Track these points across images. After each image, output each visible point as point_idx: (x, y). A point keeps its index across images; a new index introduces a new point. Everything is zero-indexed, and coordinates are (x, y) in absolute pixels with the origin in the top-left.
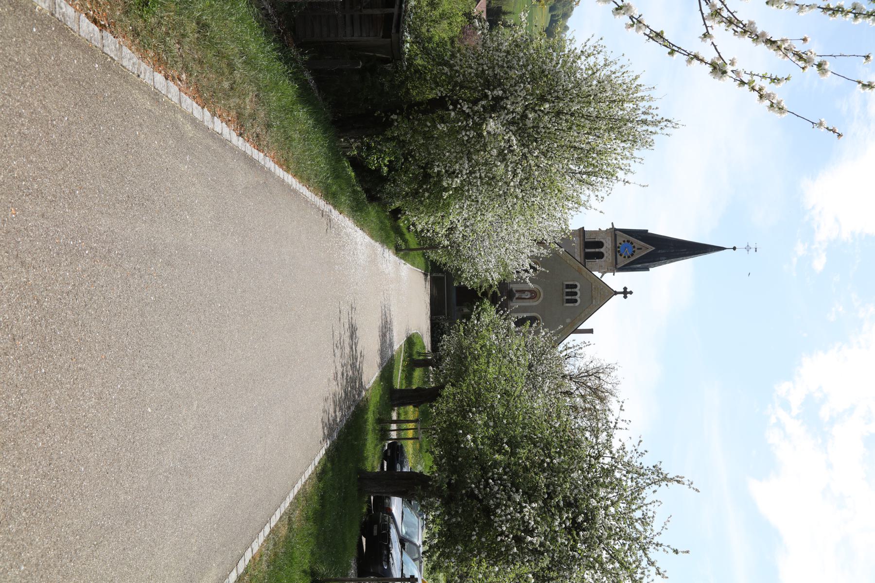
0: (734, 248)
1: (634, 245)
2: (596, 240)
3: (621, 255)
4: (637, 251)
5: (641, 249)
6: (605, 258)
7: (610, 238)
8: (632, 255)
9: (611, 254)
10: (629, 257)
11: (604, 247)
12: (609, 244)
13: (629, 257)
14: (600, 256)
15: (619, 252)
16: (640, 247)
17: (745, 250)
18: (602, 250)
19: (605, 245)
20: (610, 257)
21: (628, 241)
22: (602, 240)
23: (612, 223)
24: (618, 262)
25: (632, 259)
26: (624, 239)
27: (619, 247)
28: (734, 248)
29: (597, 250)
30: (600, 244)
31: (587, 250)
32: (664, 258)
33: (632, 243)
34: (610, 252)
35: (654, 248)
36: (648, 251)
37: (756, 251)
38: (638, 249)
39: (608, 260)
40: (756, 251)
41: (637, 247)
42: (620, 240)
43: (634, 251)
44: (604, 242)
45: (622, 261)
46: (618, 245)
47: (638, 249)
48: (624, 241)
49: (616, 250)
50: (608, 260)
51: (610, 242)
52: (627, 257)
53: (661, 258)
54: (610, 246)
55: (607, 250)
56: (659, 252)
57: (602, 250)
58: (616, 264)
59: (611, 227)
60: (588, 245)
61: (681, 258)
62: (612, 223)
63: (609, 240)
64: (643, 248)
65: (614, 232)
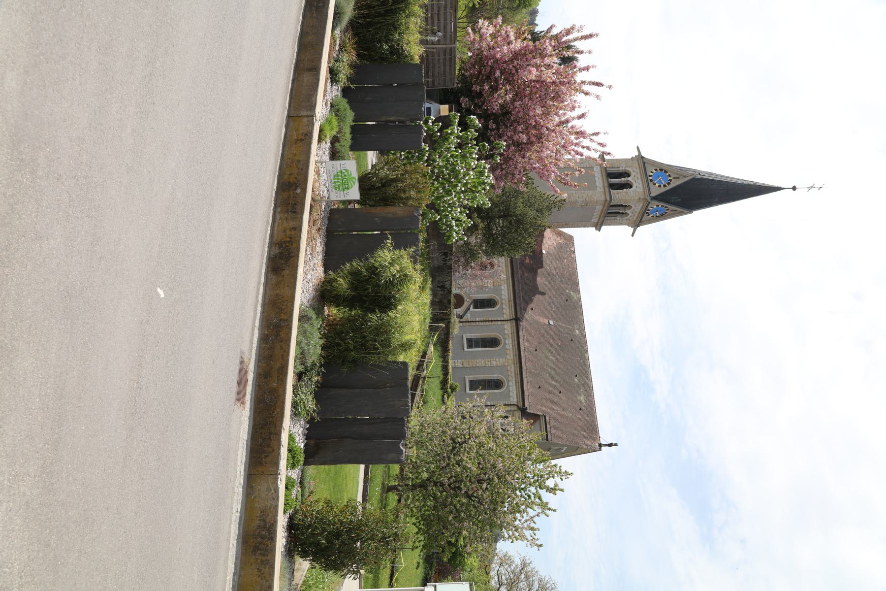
0: (794, 188)
2: (621, 169)
5: (679, 178)
6: (634, 188)
8: (669, 184)
9: (640, 182)
11: (632, 176)
13: (665, 186)
14: (628, 186)
15: (651, 180)
16: (676, 176)
18: (629, 179)
19: (633, 174)
20: (641, 186)
21: (661, 170)
22: (628, 169)
23: (638, 148)
25: (668, 188)
26: (656, 168)
27: (650, 176)
28: (794, 188)
29: (623, 179)
30: (627, 175)
33: (666, 172)
34: (640, 181)
38: (674, 178)
41: (673, 175)
44: (631, 171)
47: (674, 178)
48: (656, 170)
50: (638, 190)
51: (638, 170)
55: (636, 179)
58: (650, 193)
59: (637, 154)
60: (611, 175)
62: (638, 148)
64: (681, 177)
65: (641, 161)
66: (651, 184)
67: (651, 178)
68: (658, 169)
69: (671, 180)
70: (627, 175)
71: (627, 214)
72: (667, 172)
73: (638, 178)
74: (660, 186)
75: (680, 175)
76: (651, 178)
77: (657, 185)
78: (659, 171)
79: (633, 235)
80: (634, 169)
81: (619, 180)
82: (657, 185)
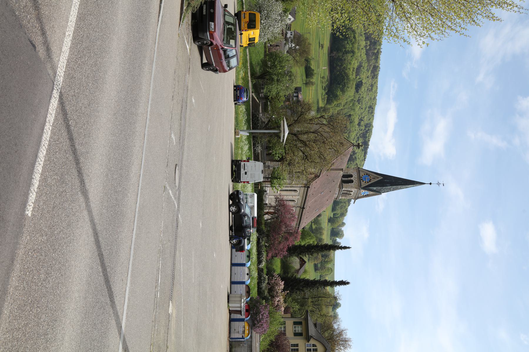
0: (430, 184)
1: (370, 176)
2: (348, 173)
3: (363, 181)
4: (372, 179)
5: (375, 178)
6: (354, 183)
7: (356, 172)
8: (370, 181)
10: (368, 182)
11: (353, 177)
12: (356, 176)
13: (368, 182)
14: (352, 181)
15: (362, 179)
16: (374, 177)
17: (437, 185)
18: (352, 178)
19: (354, 176)
20: (357, 182)
21: (367, 174)
22: (351, 173)
24: (362, 185)
25: (370, 183)
27: (361, 177)
28: (430, 184)
29: (349, 178)
30: (351, 176)
31: (344, 179)
32: (389, 185)
34: (357, 179)
35: (382, 178)
36: (379, 179)
37: (444, 185)
38: (373, 178)
39: (356, 184)
40: (444, 185)
42: (362, 174)
43: (371, 179)
45: (364, 184)
46: (361, 176)
47: (373, 178)
48: (364, 174)
49: (360, 179)
51: (356, 174)
52: (367, 182)
53: (387, 185)
54: (356, 177)
55: (355, 178)
56: (386, 180)
57: (352, 178)
58: (361, 185)
61: (399, 187)
63: (355, 173)
66: (362, 181)
67: (362, 178)
68: (365, 174)
69: (371, 179)
70: (351, 176)
71: (351, 194)
72: (369, 176)
73: (356, 178)
74: (365, 182)
75: (376, 177)
76: (362, 178)
77: (364, 181)
78: (366, 175)
79: (354, 203)
80: (355, 173)
81: (347, 179)
82: (364, 181)
